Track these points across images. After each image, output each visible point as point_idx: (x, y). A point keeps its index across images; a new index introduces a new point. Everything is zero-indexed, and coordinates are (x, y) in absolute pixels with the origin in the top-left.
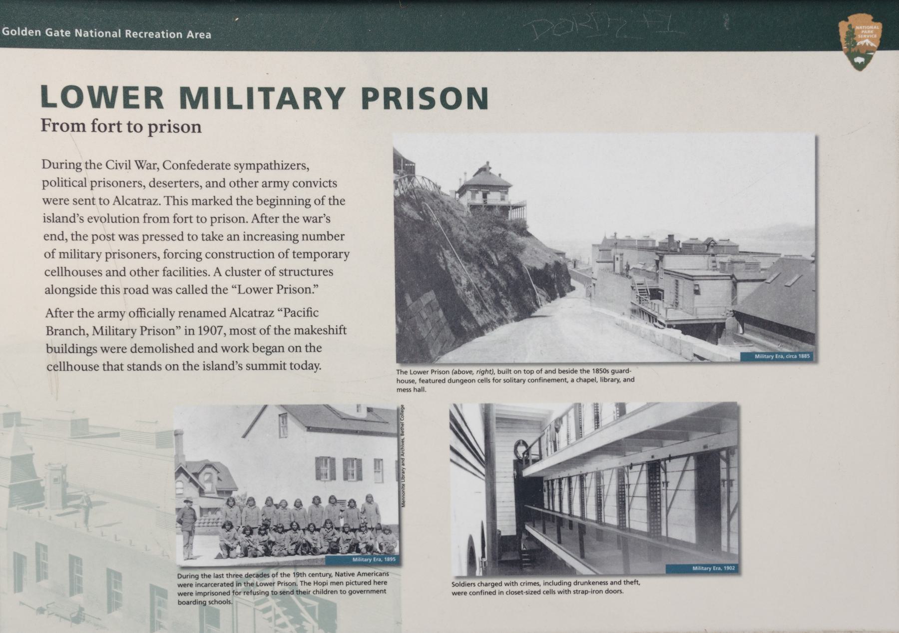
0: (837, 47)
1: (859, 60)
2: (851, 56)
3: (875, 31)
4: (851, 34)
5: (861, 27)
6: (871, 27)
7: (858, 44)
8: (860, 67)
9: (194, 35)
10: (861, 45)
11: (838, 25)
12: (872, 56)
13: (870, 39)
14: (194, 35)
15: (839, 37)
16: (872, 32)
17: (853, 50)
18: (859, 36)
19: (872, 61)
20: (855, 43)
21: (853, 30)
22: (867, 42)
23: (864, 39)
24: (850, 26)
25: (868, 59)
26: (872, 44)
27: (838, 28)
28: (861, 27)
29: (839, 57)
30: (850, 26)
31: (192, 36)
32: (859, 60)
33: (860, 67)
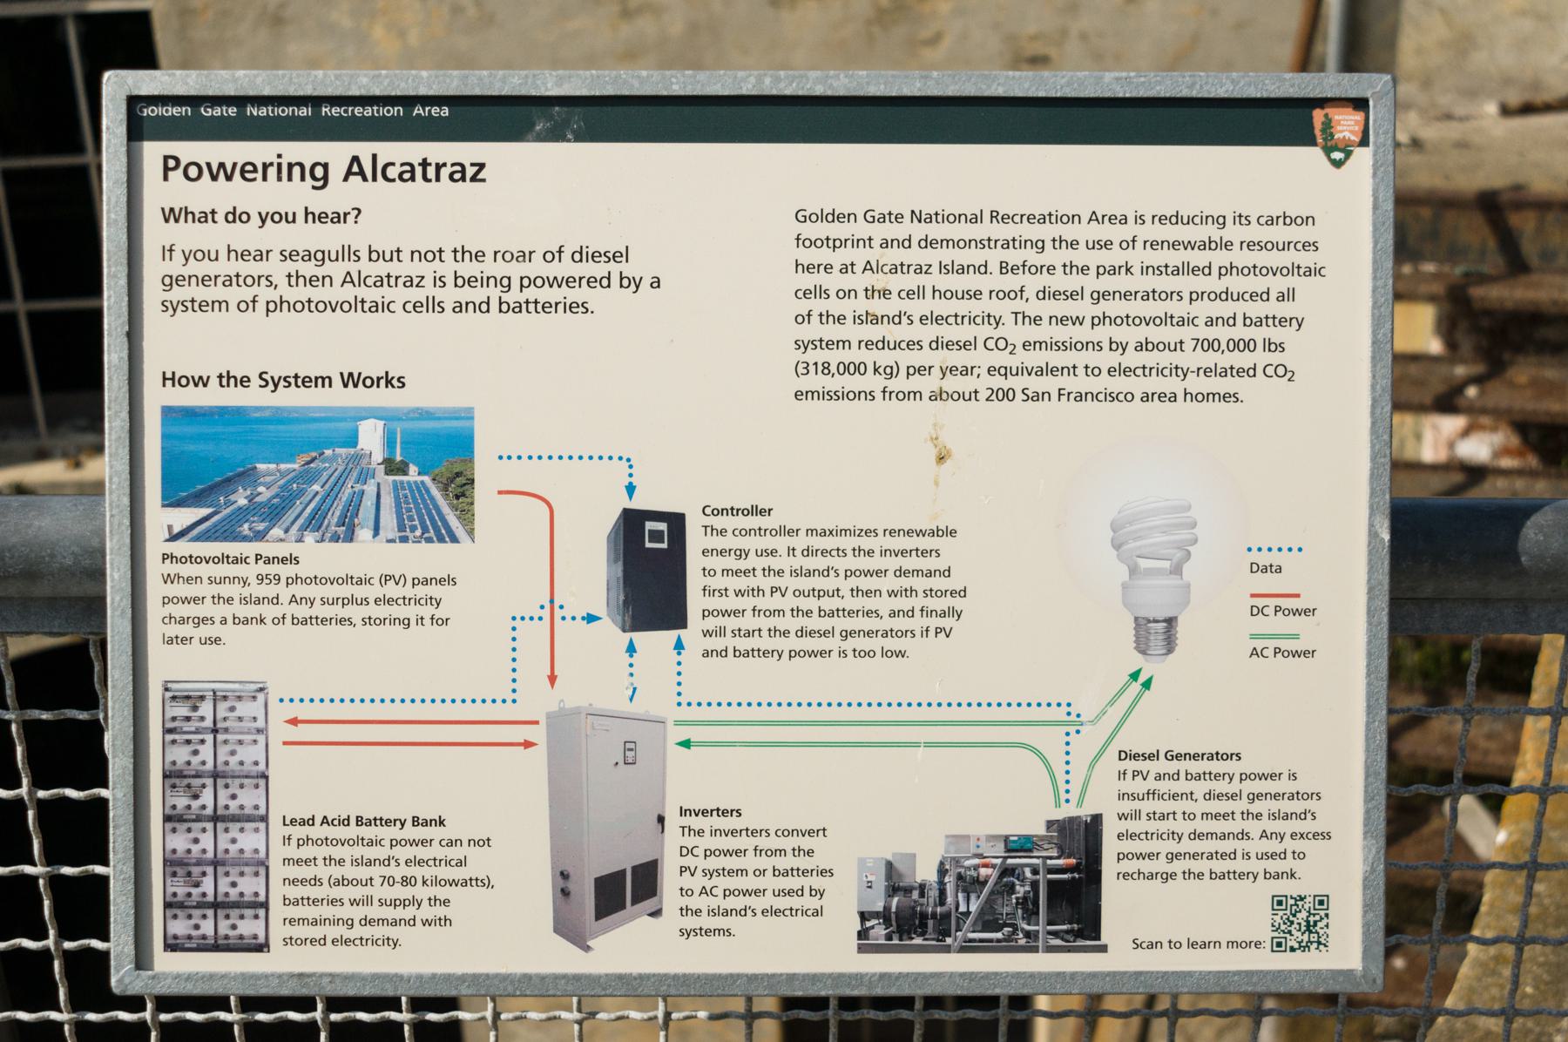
0: (1313, 143)
1: (1337, 155)
2: (1328, 150)
3: (1357, 122)
4: (1328, 125)
5: (1340, 117)
6: (1352, 117)
7: (1336, 137)
8: (1338, 164)
9: (424, 111)
10: (1338, 139)
11: (1311, 113)
12: (1352, 151)
13: (1351, 132)
14: (424, 111)
15: (1313, 128)
16: (1353, 123)
17: (1329, 144)
18: (1339, 128)
19: (1353, 158)
20: (1332, 135)
21: (1330, 120)
22: (1347, 135)
23: (1342, 131)
24: (1326, 115)
25: (1348, 154)
26: (1353, 138)
27: (1312, 118)
28: (1340, 117)
29: (1313, 154)
30: (1326, 115)
31: (421, 112)
32: (1337, 155)
33: (1338, 164)
